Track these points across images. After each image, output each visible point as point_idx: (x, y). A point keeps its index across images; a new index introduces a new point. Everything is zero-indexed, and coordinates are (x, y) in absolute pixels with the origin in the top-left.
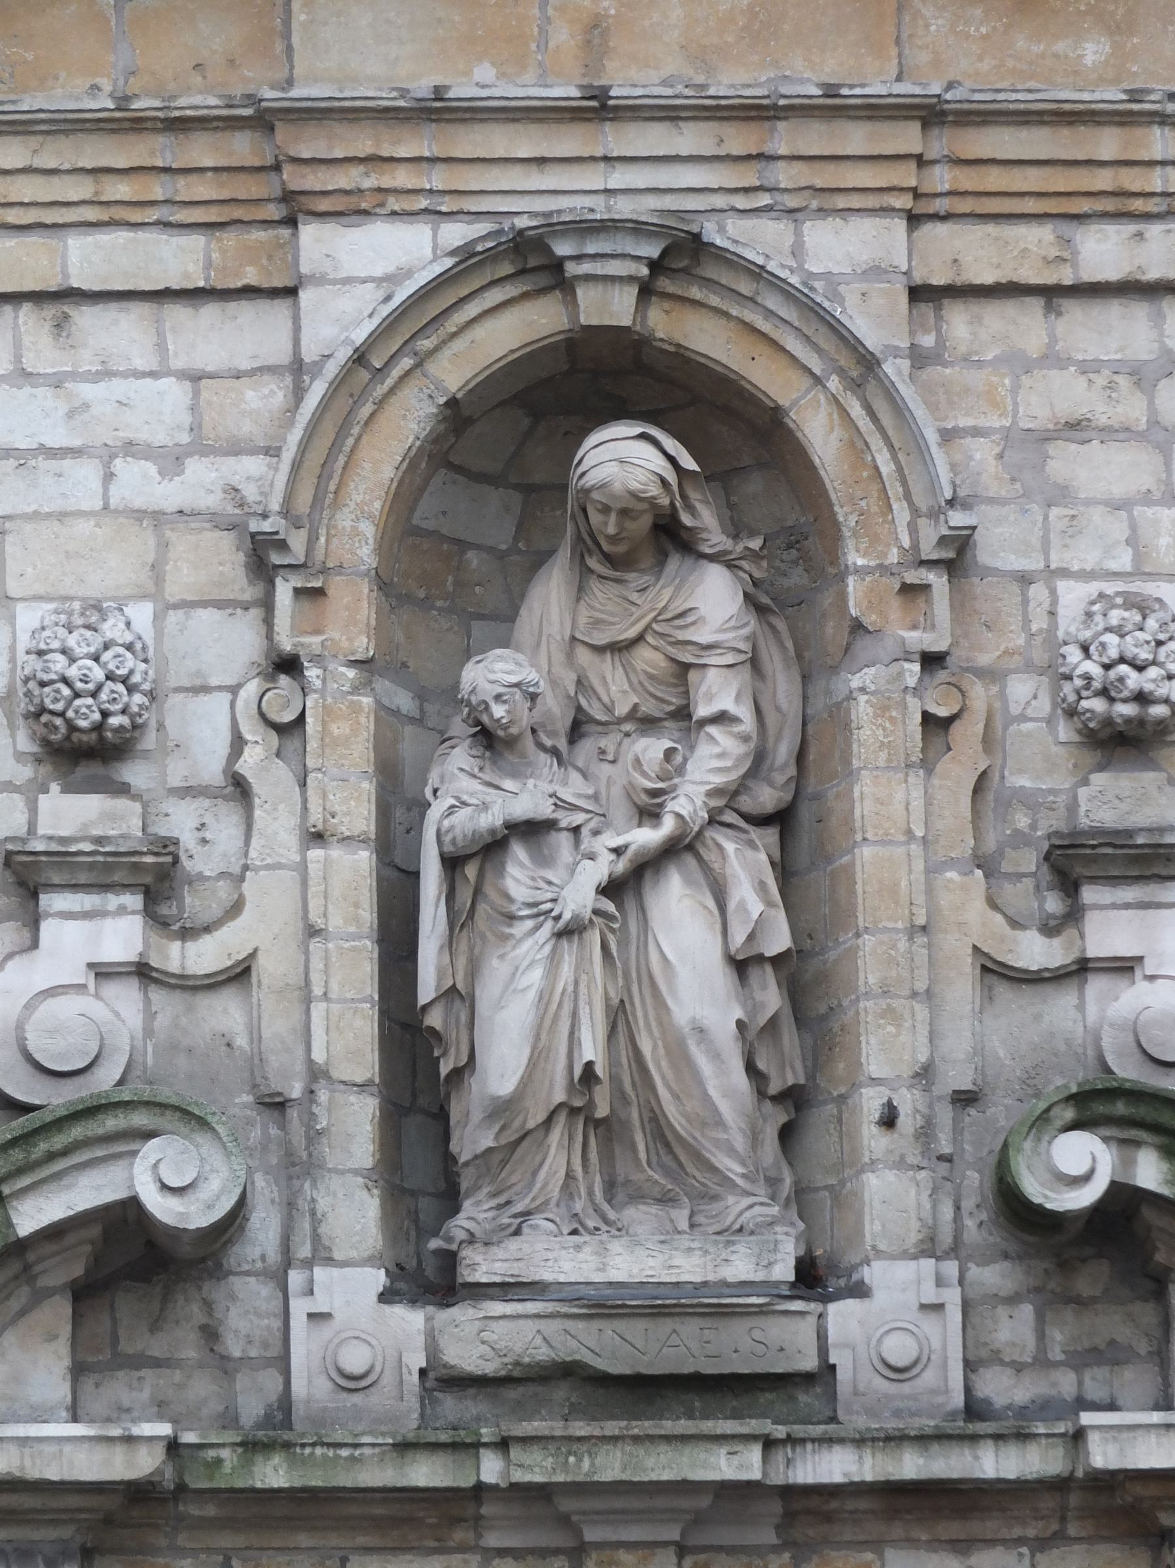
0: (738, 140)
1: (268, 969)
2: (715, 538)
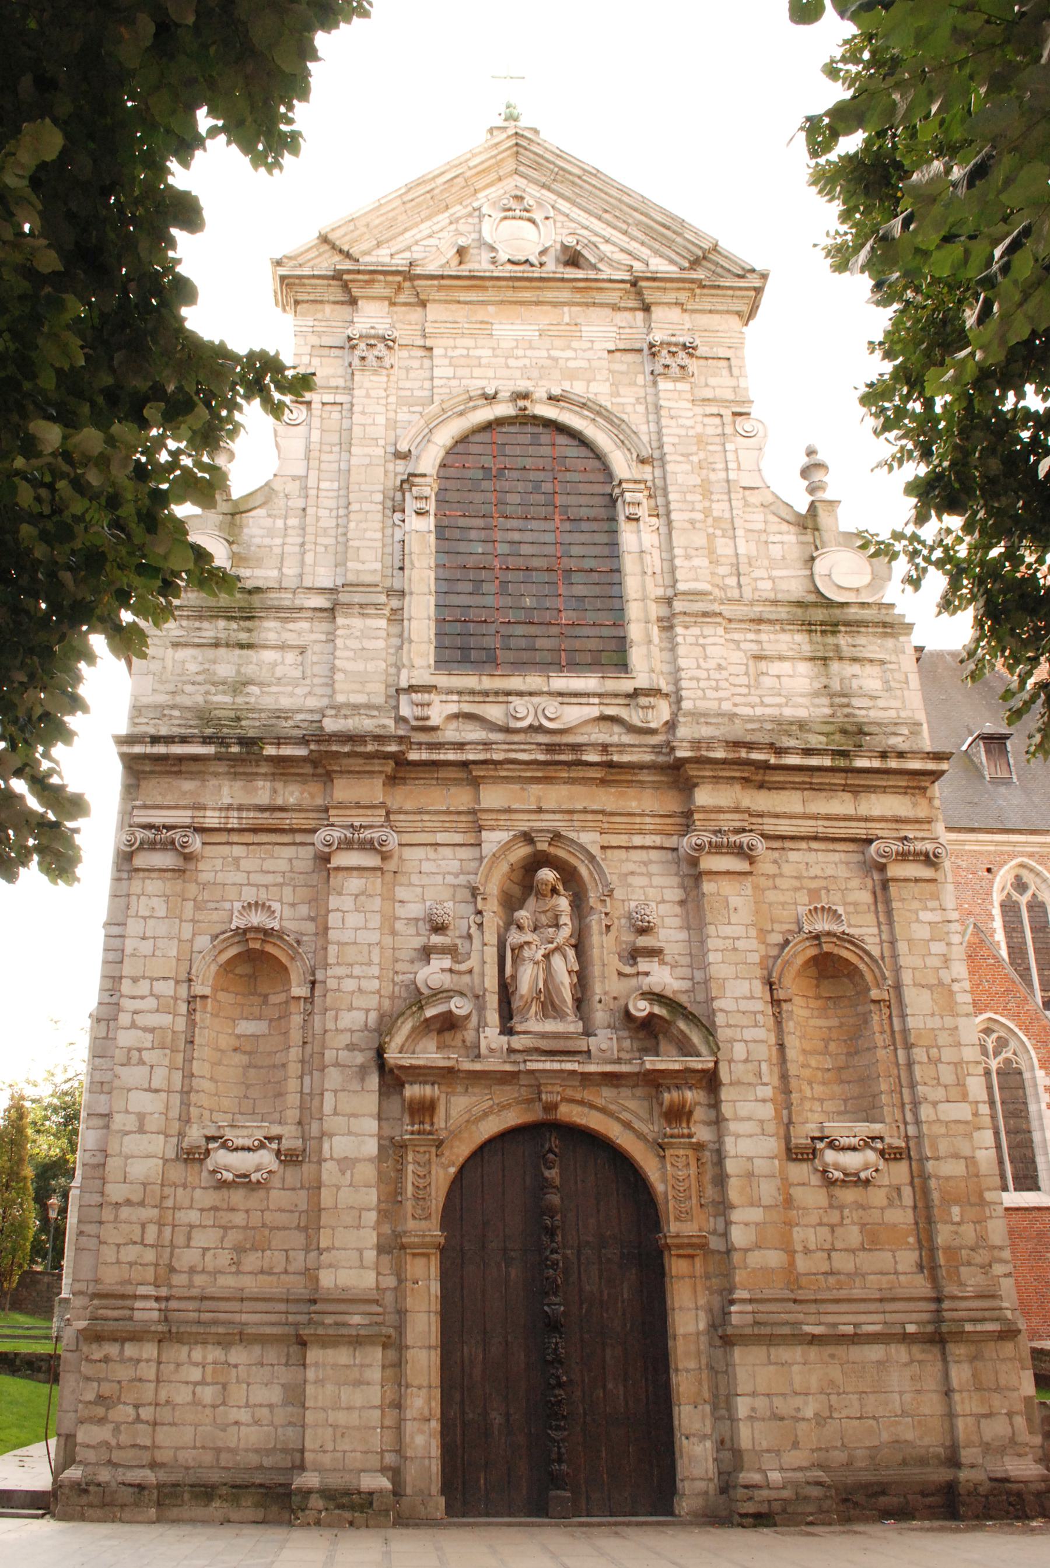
0: (567, 817)
1: (476, 970)
2: (562, 892)
